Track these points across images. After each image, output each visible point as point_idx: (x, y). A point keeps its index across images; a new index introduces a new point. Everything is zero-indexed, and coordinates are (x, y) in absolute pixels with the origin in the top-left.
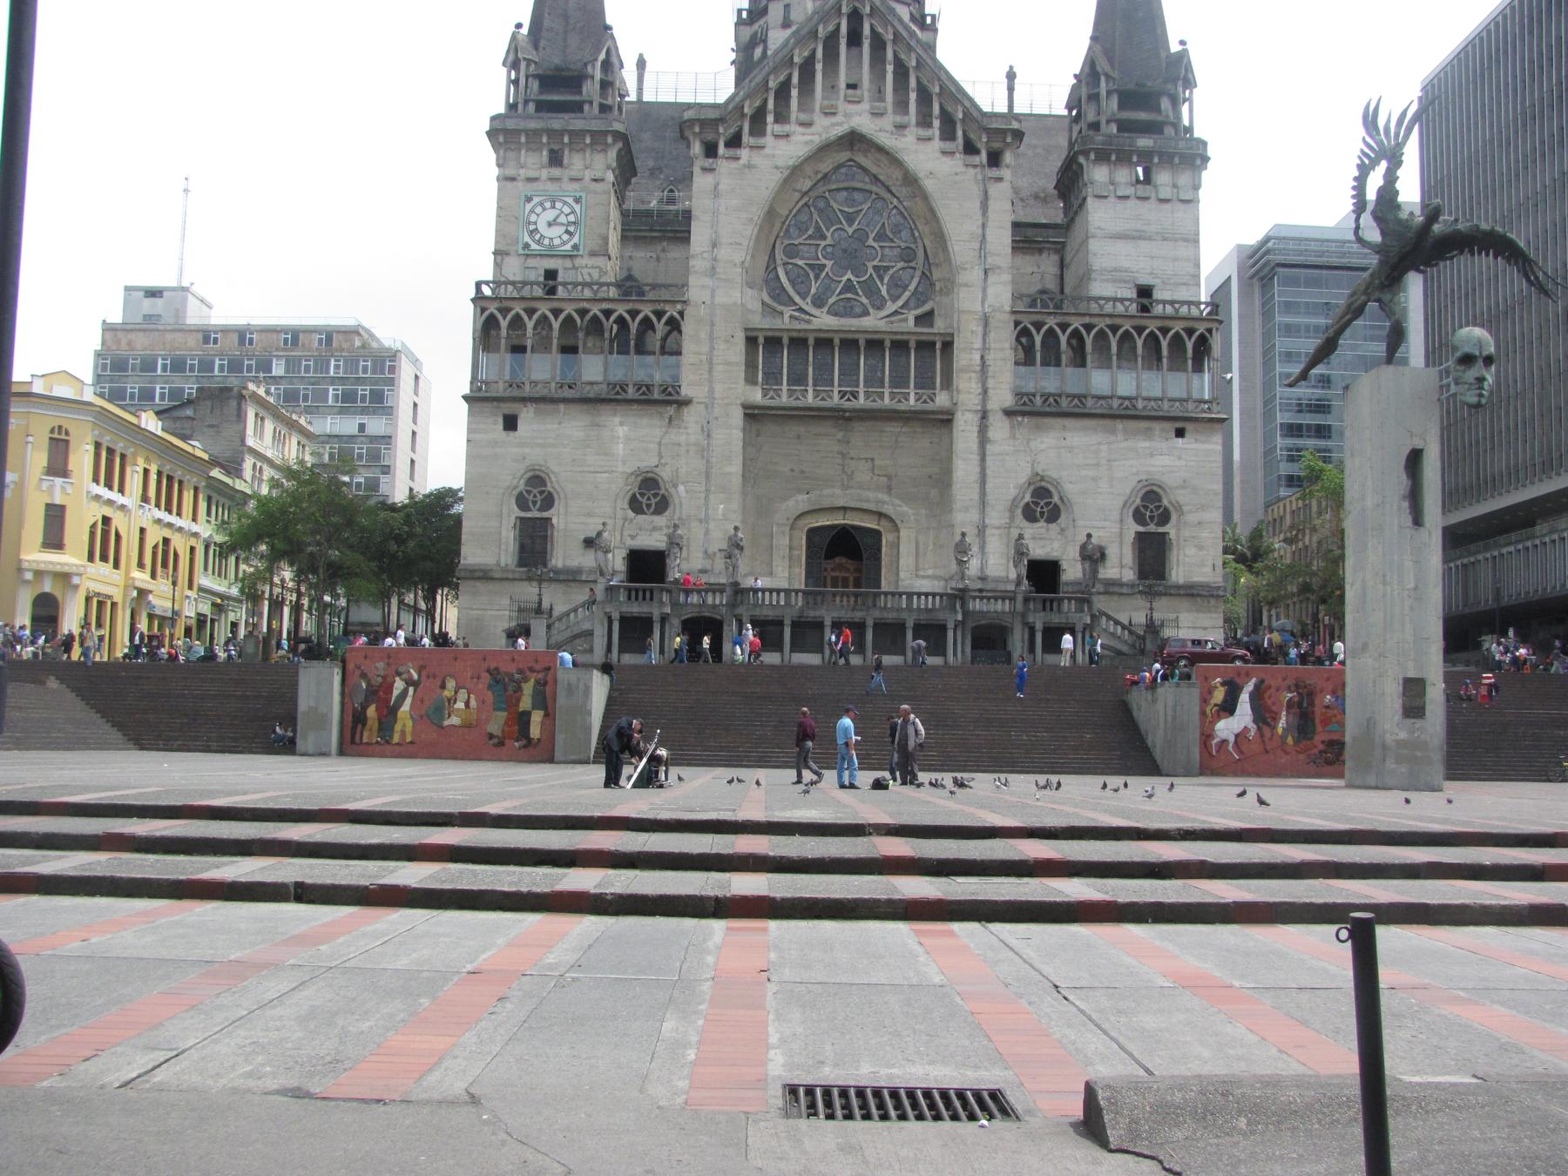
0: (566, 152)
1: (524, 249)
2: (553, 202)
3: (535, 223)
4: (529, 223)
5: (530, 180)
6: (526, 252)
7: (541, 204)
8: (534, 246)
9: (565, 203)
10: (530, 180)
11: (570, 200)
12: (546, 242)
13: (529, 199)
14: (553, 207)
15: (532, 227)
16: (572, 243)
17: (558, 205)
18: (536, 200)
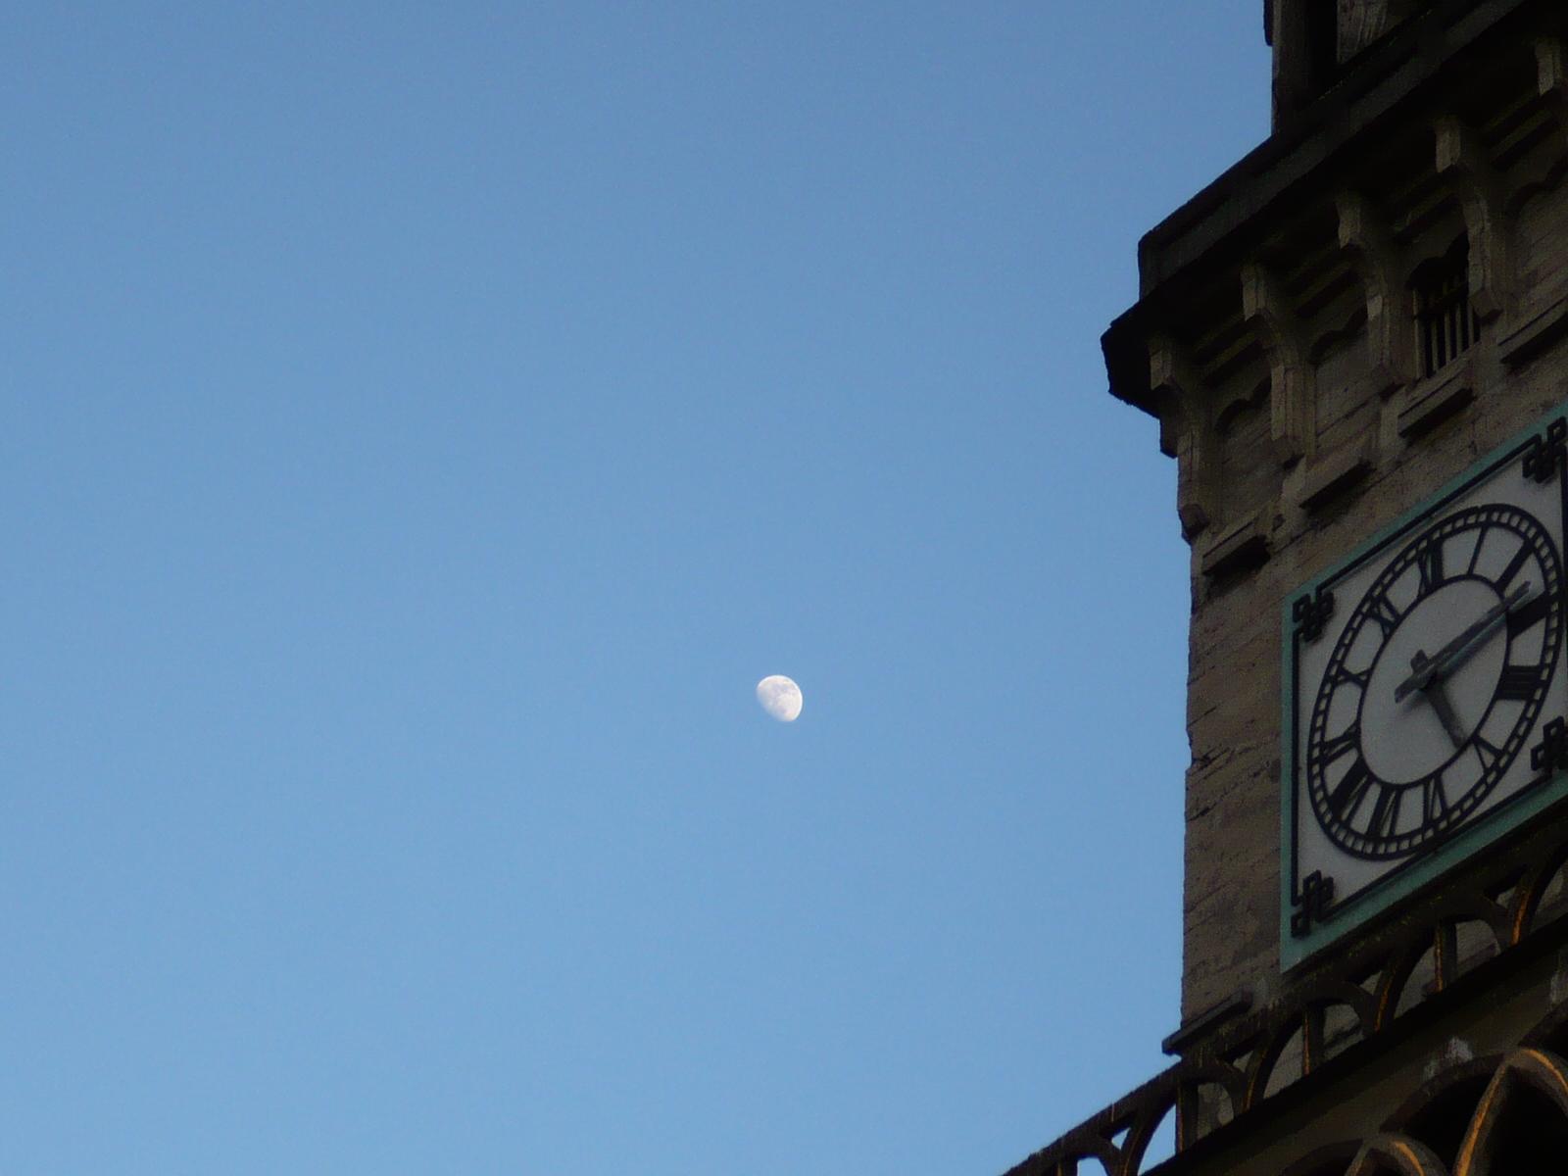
0: (1478, 222)
1: (1300, 931)
2: (1430, 554)
3: (1353, 737)
4: (1327, 753)
5: (1326, 505)
6: (1324, 937)
7: (1374, 605)
8: (1351, 875)
9: (1490, 518)
10: (1326, 505)
11: (1510, 488)
12: (1410, 815)
13: (1312, 617)
14: (1433, 583)
15: (1336, 773)
16: (1536, 737)
17: (1456, 554)
18: (1350, 596)
